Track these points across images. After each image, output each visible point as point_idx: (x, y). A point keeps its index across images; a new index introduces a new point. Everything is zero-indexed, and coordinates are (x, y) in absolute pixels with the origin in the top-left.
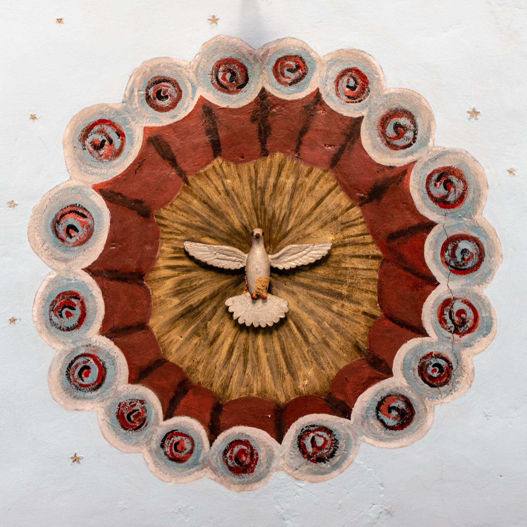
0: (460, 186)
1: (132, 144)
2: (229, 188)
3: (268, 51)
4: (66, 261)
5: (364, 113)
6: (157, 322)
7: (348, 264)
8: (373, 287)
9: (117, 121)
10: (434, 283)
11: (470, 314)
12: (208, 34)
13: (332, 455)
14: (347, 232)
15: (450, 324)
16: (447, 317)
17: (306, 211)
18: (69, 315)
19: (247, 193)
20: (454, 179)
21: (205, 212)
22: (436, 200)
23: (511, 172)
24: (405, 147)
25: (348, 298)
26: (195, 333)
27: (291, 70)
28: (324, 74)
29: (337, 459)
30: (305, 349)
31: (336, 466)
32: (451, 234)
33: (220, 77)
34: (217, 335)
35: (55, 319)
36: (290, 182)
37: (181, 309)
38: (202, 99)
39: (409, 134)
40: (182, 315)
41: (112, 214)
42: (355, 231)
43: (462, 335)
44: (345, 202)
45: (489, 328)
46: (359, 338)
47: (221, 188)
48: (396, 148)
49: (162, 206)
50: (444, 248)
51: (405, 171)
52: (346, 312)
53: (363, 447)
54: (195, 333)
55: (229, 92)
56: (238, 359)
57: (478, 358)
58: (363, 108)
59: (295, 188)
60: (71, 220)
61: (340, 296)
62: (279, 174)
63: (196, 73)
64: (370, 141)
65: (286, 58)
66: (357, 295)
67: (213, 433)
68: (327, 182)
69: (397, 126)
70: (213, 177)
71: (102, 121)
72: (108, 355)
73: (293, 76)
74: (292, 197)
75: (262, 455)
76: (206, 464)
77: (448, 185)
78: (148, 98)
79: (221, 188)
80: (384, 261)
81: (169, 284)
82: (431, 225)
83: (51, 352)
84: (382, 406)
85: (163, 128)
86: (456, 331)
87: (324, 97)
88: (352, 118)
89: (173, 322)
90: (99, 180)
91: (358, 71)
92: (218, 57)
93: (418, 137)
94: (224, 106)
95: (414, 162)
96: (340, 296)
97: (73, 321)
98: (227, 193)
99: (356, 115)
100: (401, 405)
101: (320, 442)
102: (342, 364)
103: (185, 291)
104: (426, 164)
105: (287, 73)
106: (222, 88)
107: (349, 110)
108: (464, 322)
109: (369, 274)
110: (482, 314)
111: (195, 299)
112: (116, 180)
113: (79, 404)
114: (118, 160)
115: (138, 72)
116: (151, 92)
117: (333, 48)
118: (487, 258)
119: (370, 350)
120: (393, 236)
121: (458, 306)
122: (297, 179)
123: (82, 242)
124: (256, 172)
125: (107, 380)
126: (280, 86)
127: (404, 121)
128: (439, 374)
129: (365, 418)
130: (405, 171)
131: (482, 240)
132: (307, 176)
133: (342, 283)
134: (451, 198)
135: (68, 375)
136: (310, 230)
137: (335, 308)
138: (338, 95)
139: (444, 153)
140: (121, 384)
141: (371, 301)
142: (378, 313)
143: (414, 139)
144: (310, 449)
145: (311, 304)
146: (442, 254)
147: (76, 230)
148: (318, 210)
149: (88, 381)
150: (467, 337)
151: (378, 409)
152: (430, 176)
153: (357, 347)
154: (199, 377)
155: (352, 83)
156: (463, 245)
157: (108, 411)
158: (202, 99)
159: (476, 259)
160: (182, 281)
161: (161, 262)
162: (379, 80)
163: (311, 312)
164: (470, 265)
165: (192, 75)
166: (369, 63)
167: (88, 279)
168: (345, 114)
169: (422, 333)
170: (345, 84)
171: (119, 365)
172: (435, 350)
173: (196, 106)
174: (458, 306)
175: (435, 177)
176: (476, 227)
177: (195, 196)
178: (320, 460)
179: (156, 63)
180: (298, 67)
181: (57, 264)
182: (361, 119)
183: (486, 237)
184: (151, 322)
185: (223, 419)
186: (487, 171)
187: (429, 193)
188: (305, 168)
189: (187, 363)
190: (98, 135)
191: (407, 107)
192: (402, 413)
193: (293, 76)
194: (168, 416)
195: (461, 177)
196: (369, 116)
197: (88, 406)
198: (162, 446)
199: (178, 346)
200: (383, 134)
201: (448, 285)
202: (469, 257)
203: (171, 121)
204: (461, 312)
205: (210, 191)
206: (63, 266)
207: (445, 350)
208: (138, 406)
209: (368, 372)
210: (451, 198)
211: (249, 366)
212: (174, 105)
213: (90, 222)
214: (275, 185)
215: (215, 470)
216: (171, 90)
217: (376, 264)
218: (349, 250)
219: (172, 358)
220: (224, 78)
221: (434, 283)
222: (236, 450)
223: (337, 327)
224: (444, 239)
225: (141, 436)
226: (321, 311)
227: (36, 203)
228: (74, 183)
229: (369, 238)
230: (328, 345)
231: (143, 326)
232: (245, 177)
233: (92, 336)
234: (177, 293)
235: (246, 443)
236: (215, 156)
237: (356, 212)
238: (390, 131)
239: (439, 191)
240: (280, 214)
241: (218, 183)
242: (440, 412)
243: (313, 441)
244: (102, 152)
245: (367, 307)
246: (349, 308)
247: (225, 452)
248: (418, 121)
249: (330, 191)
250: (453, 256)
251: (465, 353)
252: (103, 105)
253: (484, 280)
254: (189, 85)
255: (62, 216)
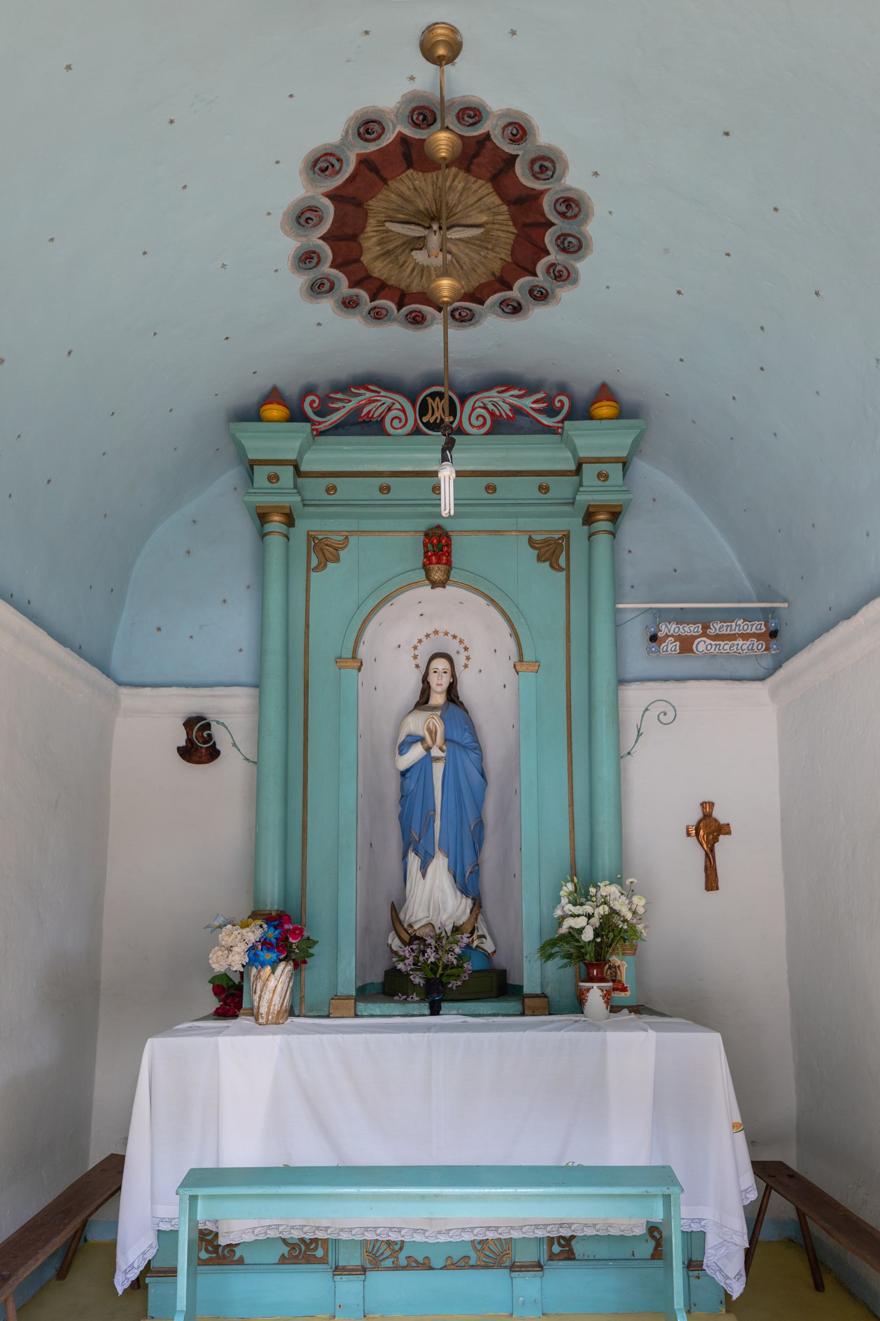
0: (576, 210)
1: (348, 165)
2: (417, 187)
3: (453, 103)
4: (306, 236)
5: (520, 153)
6: (365, 259)
7: (495, 233)
8: (509, 247)
9: (337, 153)
10: (548, 253)
11: (565, 273)
12: (408, 88)
13: (470, 320)
14: (496, 217)
15: (552, 275)
16: (551, 271)
17: (470, 203)
18: (310, 262)
19: (430, 189)
20: (573, 205)
21: (399, 201)
22: (558, 213)
23: (610, 213)
24: (544, 180)
25: (492, 250)
26: (391, 262)
27: (470, 117)
28: (494, 122)
29: (473, 321)
30: (460, 272)
31: (473, 325)
32: (564, 232)
33: (414, 118)
34: (405, 262)
35: (301, 265)
36: (461, 186)
37: (381, 252)
38: (400, 133)
39: (550, 173)
40: (383, 255)
41: (335, 207)
42: (502, 217)
43: (558, 281)
44: (498, 201)
45: (575, 282)
46: (495, 270)
47: (411, 187)
48: (538, 179)
49: (371, 199)
50: (558, 238)
51: (542, 193)
52: (489, 256)
53: (489, 318)
54: (391, 262)
55: (422, 128)
56: (417, 274)
57: (566, 294)
58: (519, 150)
59: (464, 189)
60: (308, 215)
61: (487, 248)
62: (454, 180)
63: (396, 116)
64: (521, 170)
65: (467, 109)
66: (498, 249)
67: (400, 307)
68: (488, 188)
69: (541, 167)
70: (406, 180)
71: (326, 154)
72: (335, 277)
73: (471, 121)
74: (461, 194)
75: (428, 318)
76: (395, 320)
77: (568, 207)
78: (359, 134)
79: (411, 187)
80: (518, 235)
81: (374, 240)
82: (552, 224)
83: (300, 281)
84: (503, 303)
85: (371, 153)
86: (555, 279)
87: (492, 137)
88: (510, 155)
89: (376, 258)
90: (325, 190)
91: (520, 126)
92: (414, 105)
93: (555, 175)
94: (417, 137)
95: (548, 190)
96: (487, 248)
97: (312, 265)
98: (416, 190)
99: (514, 153)
100: (515, 304)
101: (464, 314)
102: (483, 281)
103: (386, 243)
104: (557, 192)
105: (466, 119)
106: (416, 125)
107: (509, 149)
108: (561, 276)
109: (508, 240)
110: (572, 275)
111: (391, 246)
112: (337, 188)
113: (319, 301)
114: (338, 176)
115: (351, 119)
116: (362, 130)
117: (504, 107)
118: (583, 250)
119: (501, 276)
120: (525, 225)
121: (559, 268)
122: (466, 185)
123: (315, 225)
124: (437, 178)
125: (336, 287)
126: (460, 126)
127: (546, 164)
128: (541, 296)
129: (492, 306)
130: (542, 193)
131: (583, 240)
132: (474, 183)
133: (488, 242)
134: (569, 214)
135: (312, 289)
136: (471, 213)
137: (482, 254)
138: (503, 137)
139: (570, 189)
140: (343, 287)
141: (506, 254)
142: (509, 260)
143: (552, 177)
144: (457, 316)
145: (467, 251)
146: (556, 240)
147: (312, 219)
148: (479, 203)
149: (323, 290)
150: (561, 283)
151: (501, 304)
152: (557, 200)
153: (493, 274)
154: (392, 282)
155: (515, 132)
156: (570, 239)
157: (336, 301)
158: (400, 133)
159: (576, 248)
160: (383, 238)
161: (368, 229)
162: (534, 135)
163: (467, 255)
164: (572, 250)
165: (393, 117)
166: (530, 122)
167: (321, 242)
168: (506, 150)
169: (535, 275)
170: (509, 132)
171: (342, 280)
172: (540, 284)
173: (395, 138)
174: (559, 268)
175: (562, 200)
176: (582, 233)
177: (393, 192)
178: (462, 321)
179: (365, 110)
180: (475, 115)
181: (300, 239)
182: (517, 156)
183: (586, 239)
184: (362, 259)
185: (406, 300)
186: (595, 207)
187: (555, 208)
188: (473, 179)
189: (385, 276)
190: (322, 163)
191: (552, 156)
192: (514, 308)
193: (471, 121)
194: (372, 300)
195: (578, 205)
196: (523, 155)
197: (325, 300)
198: (369, 313)
199: (379, 269)
200: (531, 169)
201: (555, 256)
202: (574, 246)
203: (376, 148)
204: (559, 271)
205: (404, 189)
206: (305, 239)
207: (547, 286)
208: (355, 298)
209: (498, 286)
210: (569, 214)
211: (424, 278)
212: (378, 138)
213: (320, 214)
214: (450, 187)
215: (400, 323)
216: (376, 127)
217: (513, 236)
218: (496, 226)
219: (376, 274)
220: (417, 118)
221: (548, 253)
222: (413, 314)
223: (482, 263)
224: (559, 233)
225: (356, 310)
226: (473, 254)
227: (285, 209)
228: (309, 194)
229: (511, 223)
230: (475, 271)
231: (358, 261)
232: (429, 181)
233: (326, 269)
234: (379, 244)
235: (420, 312)
236: (408, 168)
237: (505, 208)
238: (536, 167)
239: (563, 208)
240: (451, 203)
241: (409, 184)
242: (538, 314)
243: (460, 314)
244: (327, 173)
245: (503, 256)
246: (491, 255)
247: (407, 315)
248: (557, 166)
249: (488, 194)
250: (563, 243)
251: (558, 290)
252: (325, 145)
253: (579, 259)
254: (390, 124)
255: (303, 213)
